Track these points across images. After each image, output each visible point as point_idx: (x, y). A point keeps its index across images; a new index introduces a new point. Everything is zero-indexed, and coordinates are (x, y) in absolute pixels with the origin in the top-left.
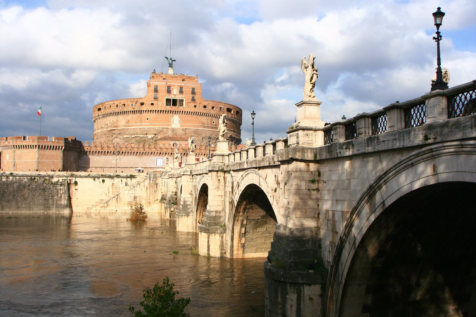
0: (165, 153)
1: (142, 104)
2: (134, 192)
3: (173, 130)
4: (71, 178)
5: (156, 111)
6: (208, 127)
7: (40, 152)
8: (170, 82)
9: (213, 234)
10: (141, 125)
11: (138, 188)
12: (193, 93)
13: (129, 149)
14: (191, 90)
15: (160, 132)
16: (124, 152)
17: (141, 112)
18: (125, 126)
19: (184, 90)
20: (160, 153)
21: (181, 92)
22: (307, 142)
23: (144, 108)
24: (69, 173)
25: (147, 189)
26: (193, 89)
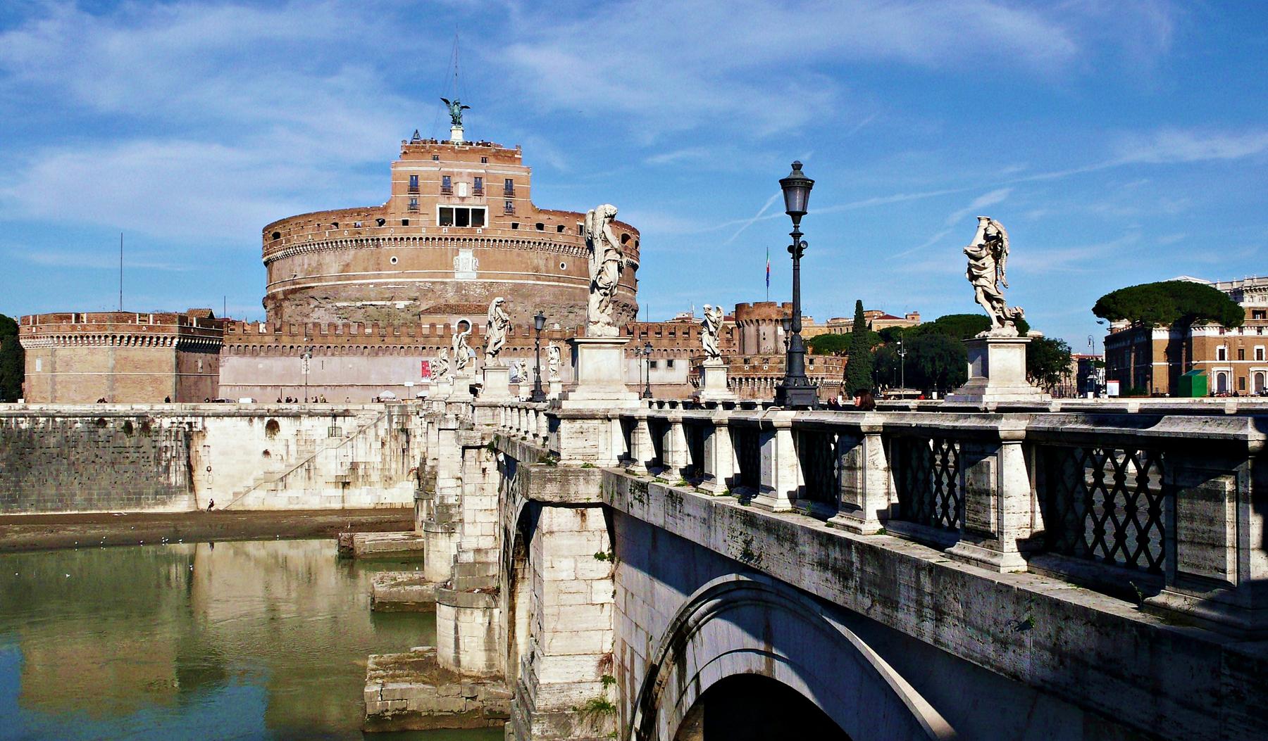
2: (350, 454)
3: (459, 287)
4: (193, 419)
6: (548, 279)
7: (118, 352)
8: (450, 166)
9: (468, 611)
10: (379, 276)
11: (360, 442)
15: (427, 292)
18: (339, 278)
19: (484, 184)
21: (478, 190)
22: (580, 451)
23: (386, 232)
24: (189, 405)
25: (383, 444)
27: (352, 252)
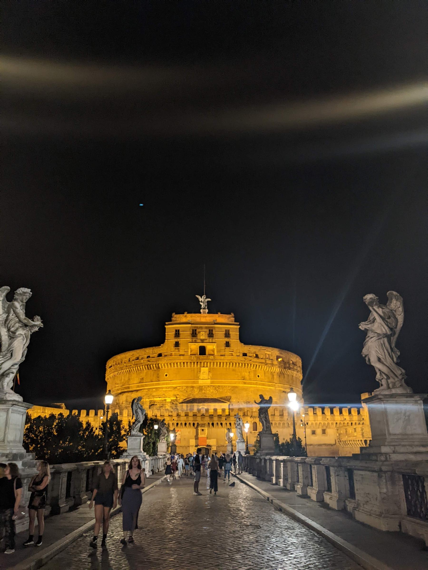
3: (201, 388)
18: (138, 387)
20: (177, 424)
27: (145, 371)
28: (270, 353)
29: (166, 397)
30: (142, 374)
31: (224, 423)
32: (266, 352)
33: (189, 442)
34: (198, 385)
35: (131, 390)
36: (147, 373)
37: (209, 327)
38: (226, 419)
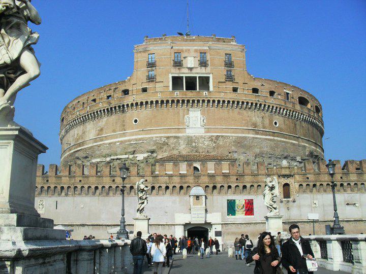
0: (164, 186)
1: (126, 92)
3: (190, 140)
5: (152, 102)
6: (265, 133)
10: (124, 135)
12: (229, 64)
13: (78, 179)
14: (223, 58)
16: (66, 186)
17: (122, 108)
19: (208, 57)
21: (203, 64)
23: (129, 100)
26: (228, 55)
28: (291, 93)
29: (136, 154)
30: (100, 123)
31: (233, 186)
32: (285, 91)
33: (173, 217)
34: (184, 134)
35: (87, 146)
36: (107, 119)
37: (200, 50)
38: (237, 179)
